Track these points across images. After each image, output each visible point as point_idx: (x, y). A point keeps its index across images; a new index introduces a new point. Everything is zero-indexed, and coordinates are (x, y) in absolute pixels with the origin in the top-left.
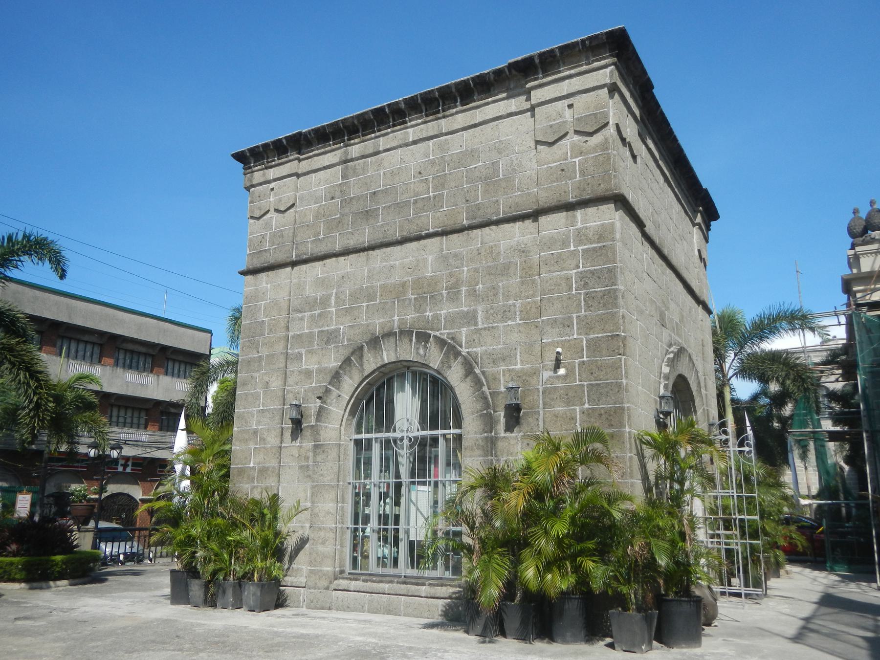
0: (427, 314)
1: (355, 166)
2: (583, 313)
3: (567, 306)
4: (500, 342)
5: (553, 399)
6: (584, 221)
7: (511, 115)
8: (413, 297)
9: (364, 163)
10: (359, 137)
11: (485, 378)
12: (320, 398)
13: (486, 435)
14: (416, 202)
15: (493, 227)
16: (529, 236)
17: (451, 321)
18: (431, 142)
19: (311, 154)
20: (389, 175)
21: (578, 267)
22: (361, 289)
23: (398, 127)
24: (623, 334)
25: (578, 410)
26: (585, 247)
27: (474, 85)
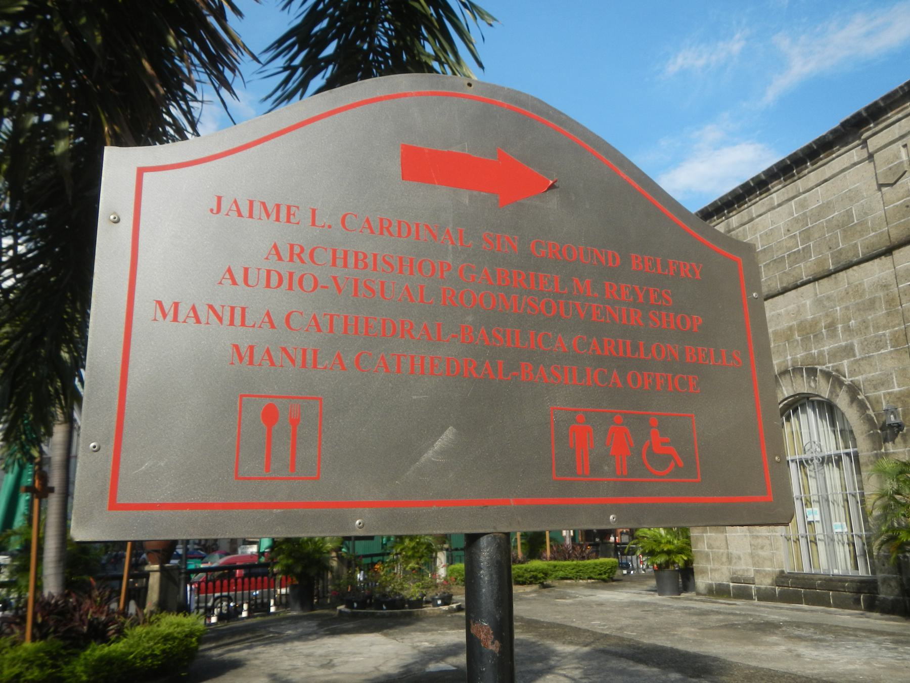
0: (813, 351)
1: (737, 233)
4: (877, 369)
7: (855, 164)
8: (799, 338)
9: (744, 230)
10: (735, 209)
13: (875, 452)
14: (789, 256)
15: (855, 268)
16: (887, 271)
17: (835, 355)
18: (793, 202)
27: (817, 146)
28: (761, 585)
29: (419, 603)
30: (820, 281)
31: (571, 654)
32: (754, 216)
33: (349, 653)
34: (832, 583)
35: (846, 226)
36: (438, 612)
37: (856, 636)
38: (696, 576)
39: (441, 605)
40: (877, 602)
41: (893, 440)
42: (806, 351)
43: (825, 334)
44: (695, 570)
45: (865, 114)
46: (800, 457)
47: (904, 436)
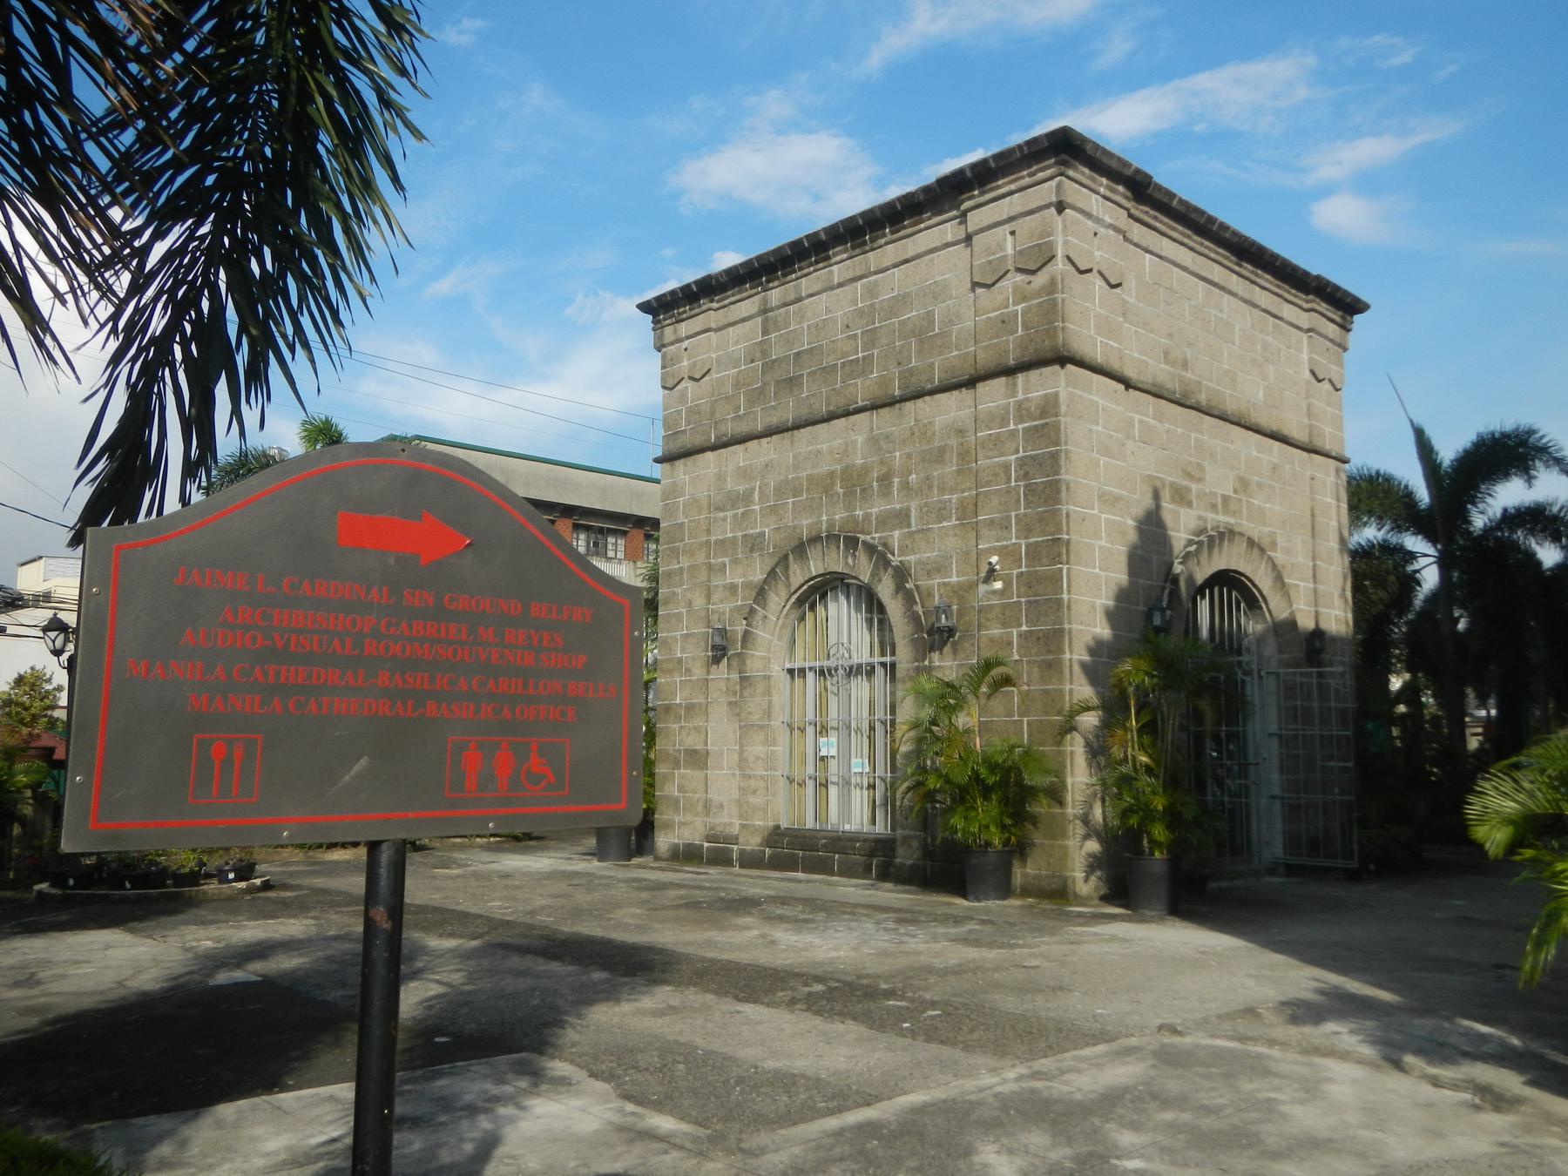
2: (1022, 511)
3: (1006, 502)
5: (988, 620)
6: (1026, 390)
7: (948, 245)
10: (778, 278)
11: (919, 594)
12: (745, 619)
14: (844, 364)
15: (927, 398)
16: (966, 411)
17: (886, 521)
18: (859, 284)
19: (726, 302)
20: (813, 329)
21: (1017, 451)
22: (786, 481)
23: (821, 265)
24: (1066, 537)
25: (1015, 633)
26: (1027, 425)
27: (902, 207)
28: (747, 845)
29: (194, 878)
30: (880, 410)
31: (450, 950)
32: (803, 294)
33: (66, 962)
34: (840, 843)
35: (924, 335)
36: (229, 892)
37: (854, 914)
38: (656, 833)
39: (235, 880)
40: (892, 869)
41: (941, 649)
42: (847, 511)
43: (876, 489)
44: (656, 825)
45: (969, 174)
46: (822, 664)
47: (955, 644)
